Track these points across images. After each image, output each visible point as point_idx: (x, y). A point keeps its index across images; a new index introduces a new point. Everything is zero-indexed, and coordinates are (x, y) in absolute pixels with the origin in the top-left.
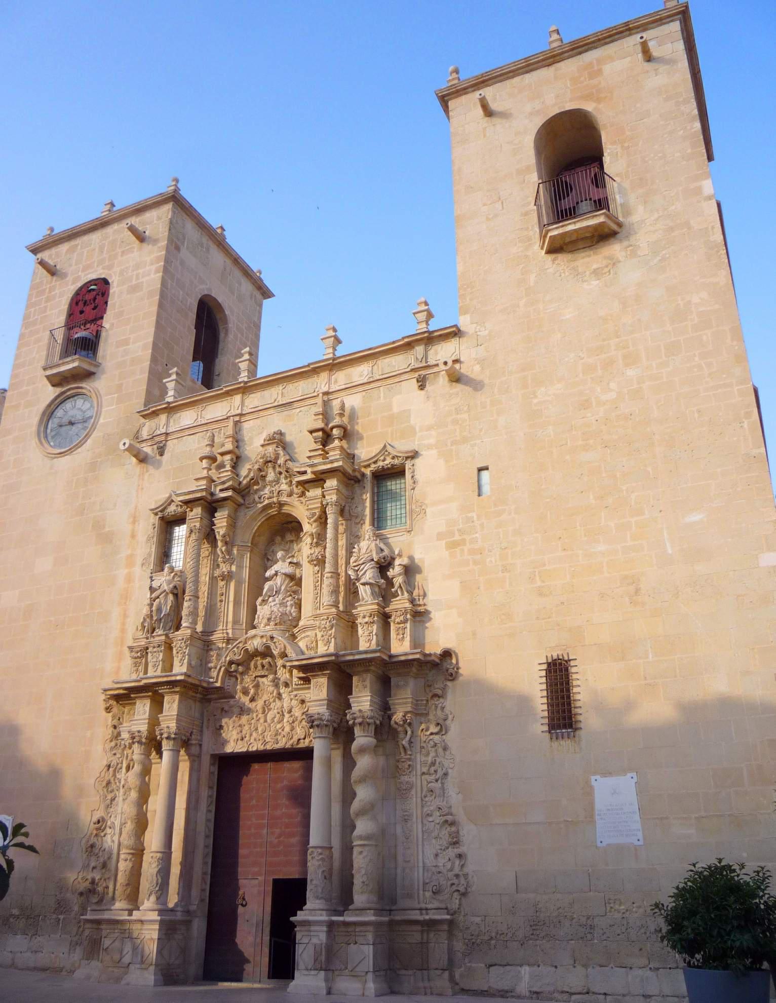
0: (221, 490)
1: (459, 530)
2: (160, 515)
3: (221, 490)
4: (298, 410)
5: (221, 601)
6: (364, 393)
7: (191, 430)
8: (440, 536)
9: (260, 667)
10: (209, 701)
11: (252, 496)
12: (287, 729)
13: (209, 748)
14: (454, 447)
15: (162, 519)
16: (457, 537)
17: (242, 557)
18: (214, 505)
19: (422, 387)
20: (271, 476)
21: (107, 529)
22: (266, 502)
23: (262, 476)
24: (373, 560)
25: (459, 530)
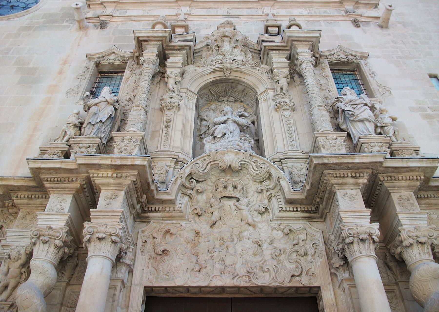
0: (179, 41)
1: (430, 108)
2: (97, 60)
3: (179, 41)
4: (245, 22)
5: (167, 127)
6: (306, 22)
7: (138, 19)
8: (412, 109)
9: (230, 188)
10: (147, 220)
11: (203, 59)
12: (271, 264)
13: (145, 274)
14: (400, 60)
15: (97, 65)
16: (429, 112)
17: (189, 99)
18: (167, 52)
19: (357, 26)
20: (227, 47)
21: (31, 66)
22: (218, 66)
23: (218, 46)
24: (366, 105)
25: (430, 108)
